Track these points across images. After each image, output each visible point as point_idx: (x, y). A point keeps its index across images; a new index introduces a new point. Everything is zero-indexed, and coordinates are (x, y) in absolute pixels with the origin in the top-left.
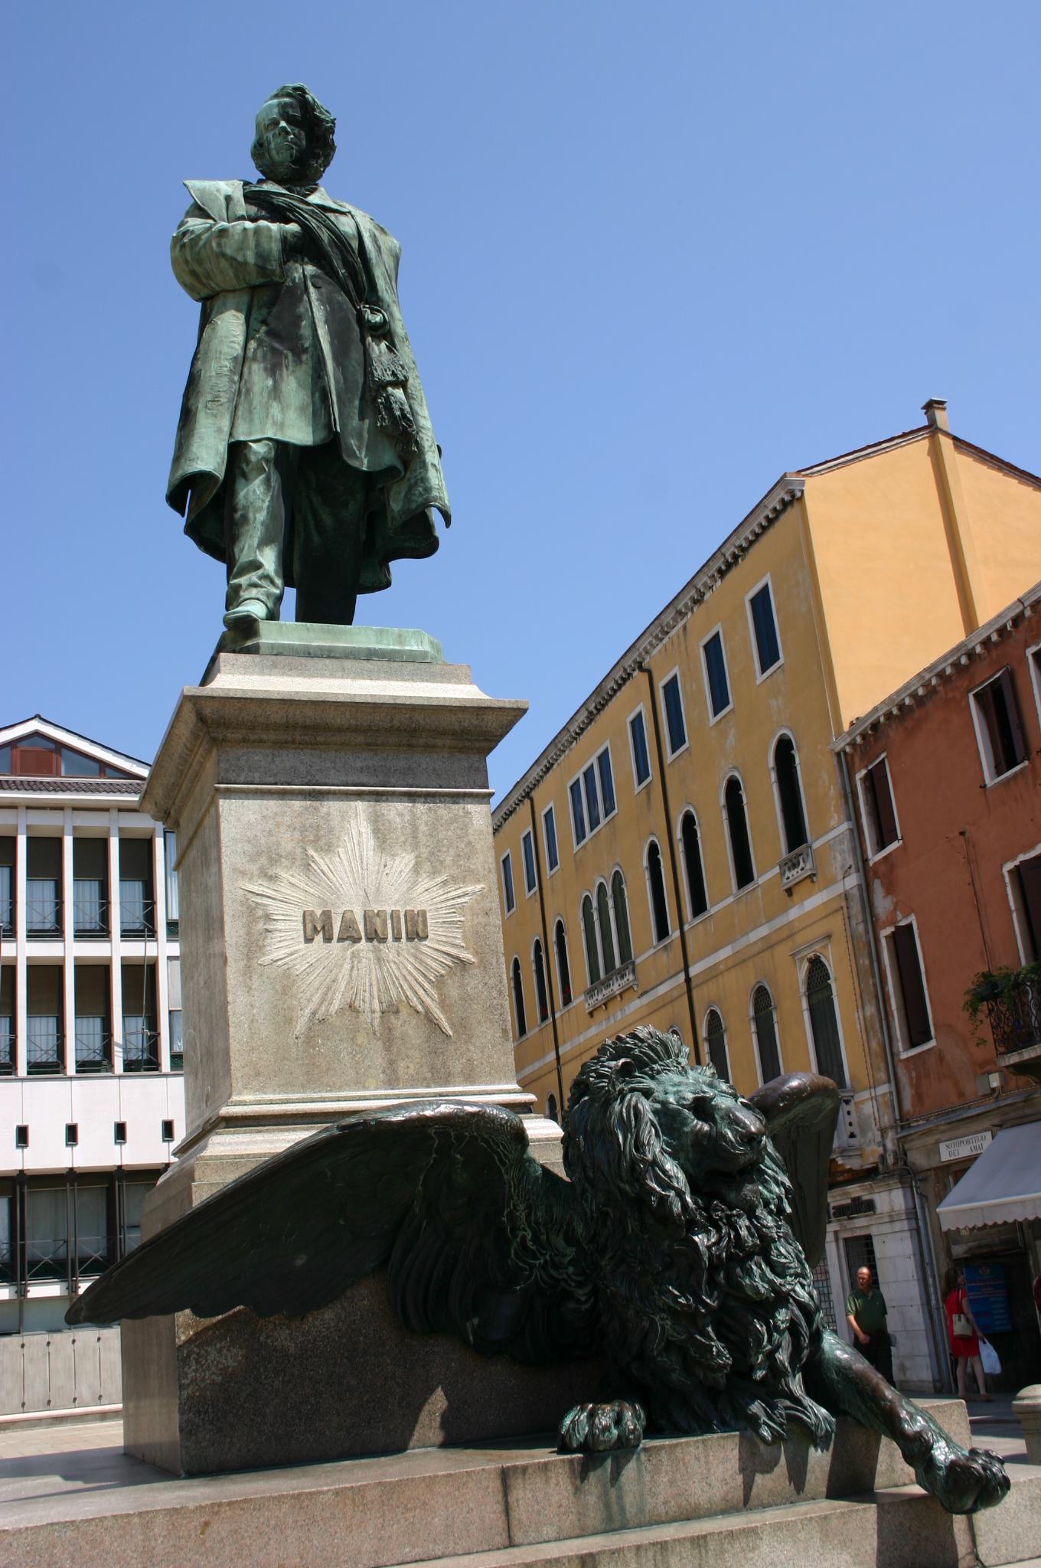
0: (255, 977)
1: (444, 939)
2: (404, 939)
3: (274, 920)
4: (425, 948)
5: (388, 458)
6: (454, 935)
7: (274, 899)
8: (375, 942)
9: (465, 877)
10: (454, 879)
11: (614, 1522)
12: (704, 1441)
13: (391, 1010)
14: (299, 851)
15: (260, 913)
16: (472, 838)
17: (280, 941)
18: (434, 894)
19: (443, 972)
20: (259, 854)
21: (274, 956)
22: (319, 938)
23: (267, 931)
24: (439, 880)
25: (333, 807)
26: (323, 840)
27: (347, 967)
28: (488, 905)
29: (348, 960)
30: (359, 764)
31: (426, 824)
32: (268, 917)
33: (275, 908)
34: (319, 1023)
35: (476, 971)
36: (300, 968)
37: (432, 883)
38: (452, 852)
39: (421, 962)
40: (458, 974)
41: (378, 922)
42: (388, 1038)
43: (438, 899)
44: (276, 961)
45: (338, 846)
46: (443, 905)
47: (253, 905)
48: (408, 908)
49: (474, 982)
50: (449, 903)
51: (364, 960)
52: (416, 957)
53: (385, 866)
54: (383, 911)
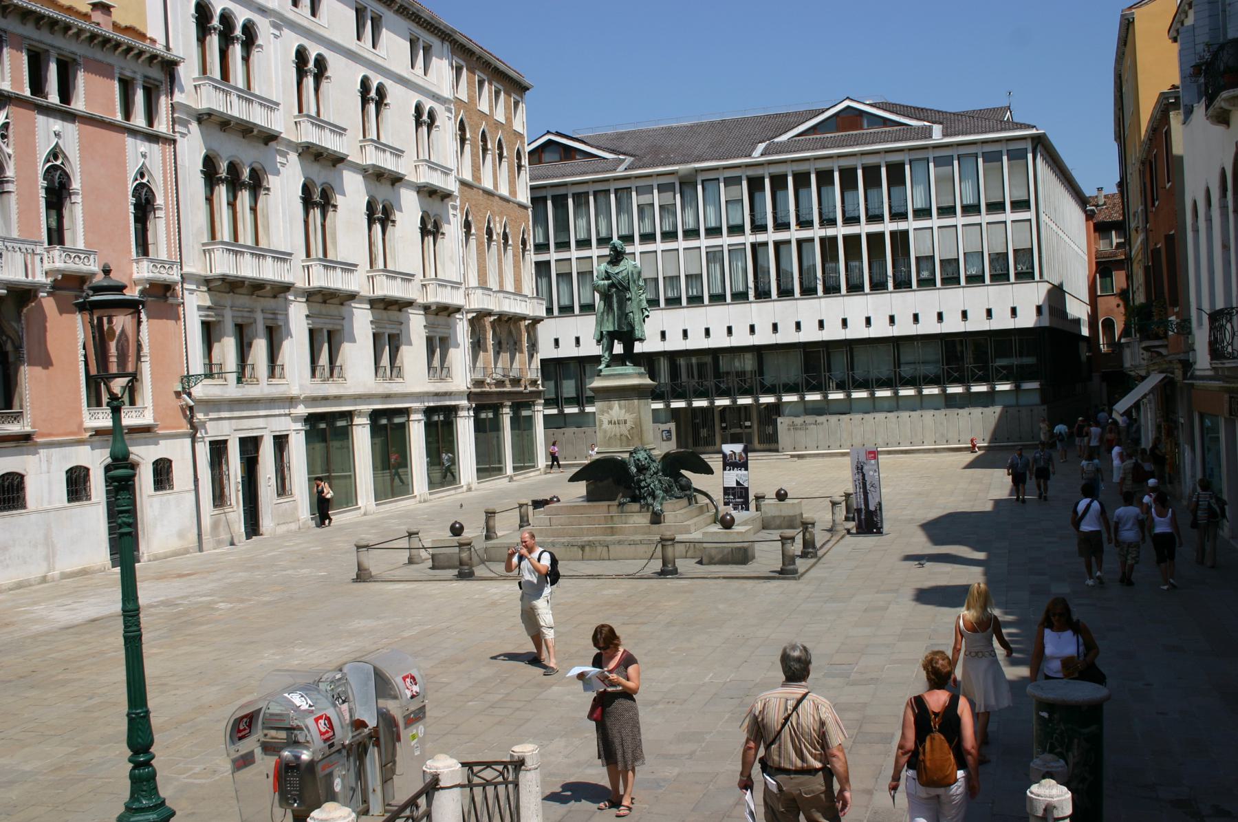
5: (629, 328)
11: (622, 512)
12: (609, 506)
13: (621, 435)
25: (612, 402)
26: (611, 408)
34: (610, 438)
42: (621, 440)
49: (635, 431)
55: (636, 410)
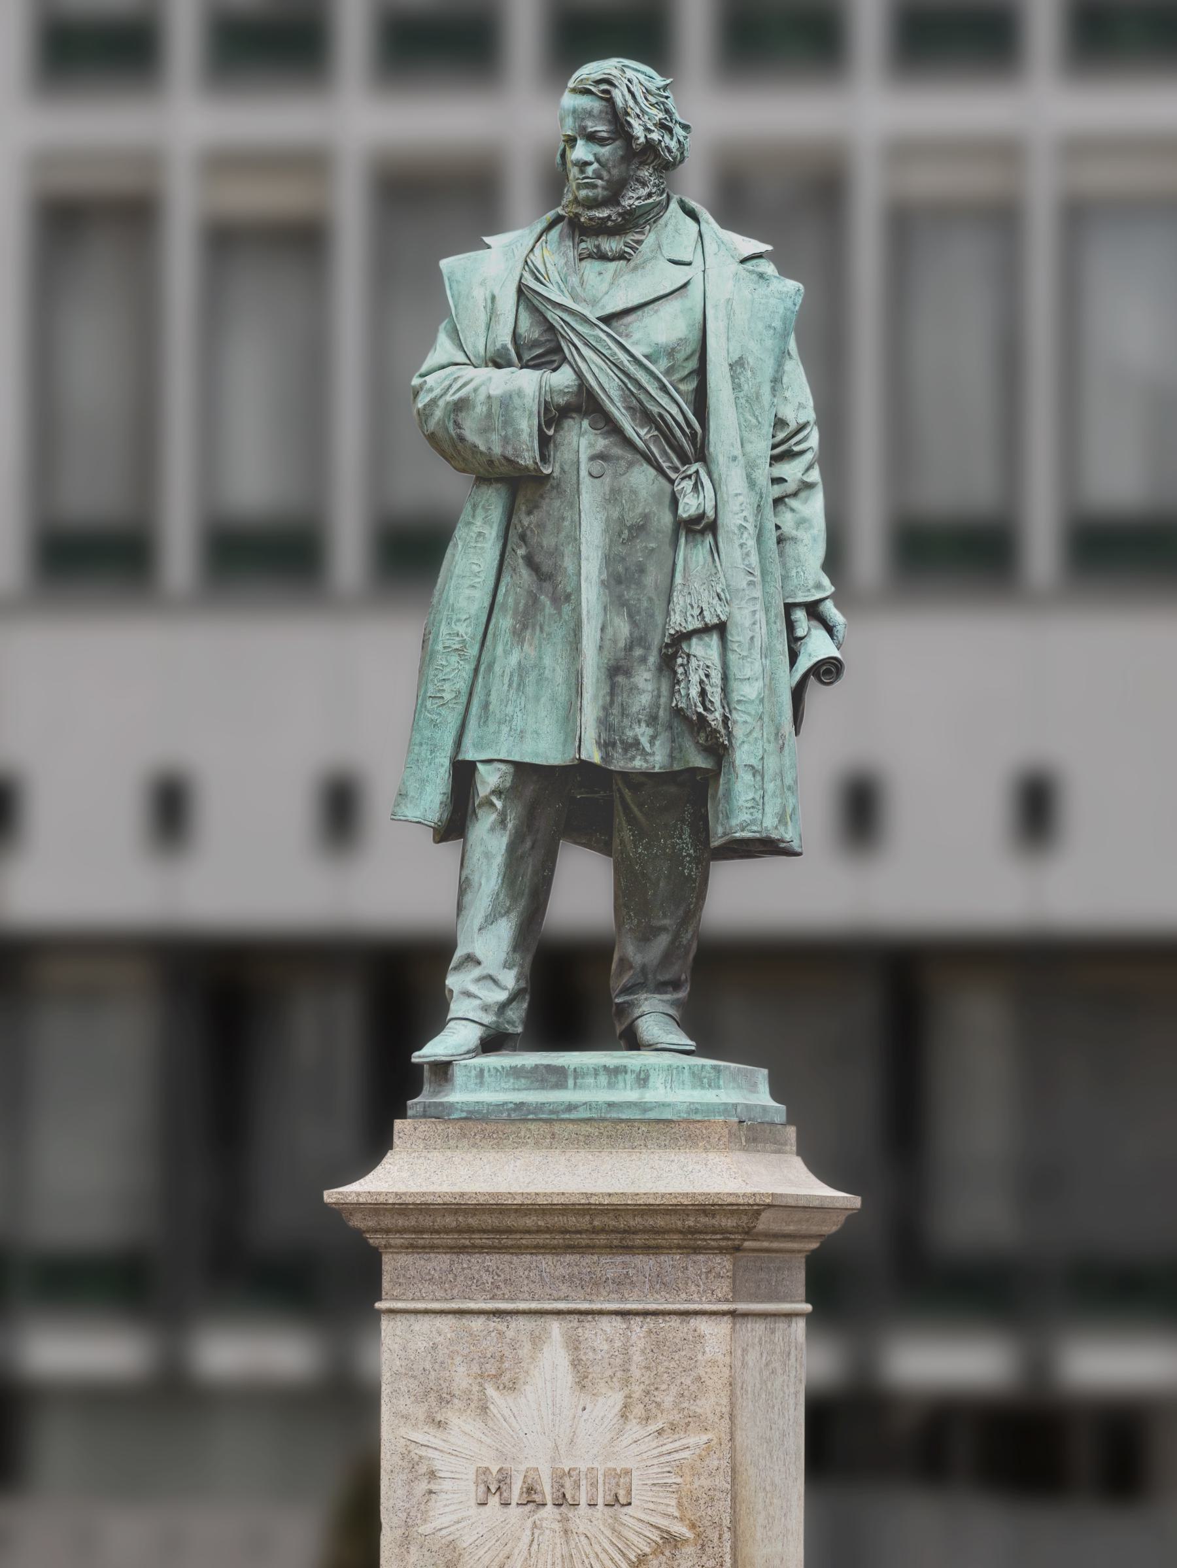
0: (413, 1549)
1: (652, 1506)
2: (600, 1506)
3: (440, 1478)
4: (626, 1518)
6: (667, 1501)
7: (441, 1451)
8: (563, 1508)
9: (688, 1424)
10: (673, 1427)
14: (475, 1388)
15: (423, 1469)
16: (701, 1372)
17: (446, 1505)
18: (643, 1448)
19: (647, 1550)
20: (426, 1394)
21: (437, 1524)
22: (494, 1501)
23: (431, 1492)
24: (653, 1427)
27: (526, 1537)
28: (716, 1463)
29: (529, 1533)
30: (561, 1271)
31: (643, 1352)
32: (432, 1475)
33: (442, 1464)
35: (689, 1550)
36: (467, 1540)
37: (644, 1433)
38: (674, 1390)
39: (620, 1536)
40: (667, 1553)
41: (568, 1483)
43: (649, 1453)
44: (441, 1529)
45: (526, 1383)
46: (655, 1461)
47: (416, 1458)
48: (610, 1465)
50: (662, 1459)
51: (547, 1532)
52: (614, 1530)
53: (584, 1409)
54: (574, 1469)
55: (710, 1404)
